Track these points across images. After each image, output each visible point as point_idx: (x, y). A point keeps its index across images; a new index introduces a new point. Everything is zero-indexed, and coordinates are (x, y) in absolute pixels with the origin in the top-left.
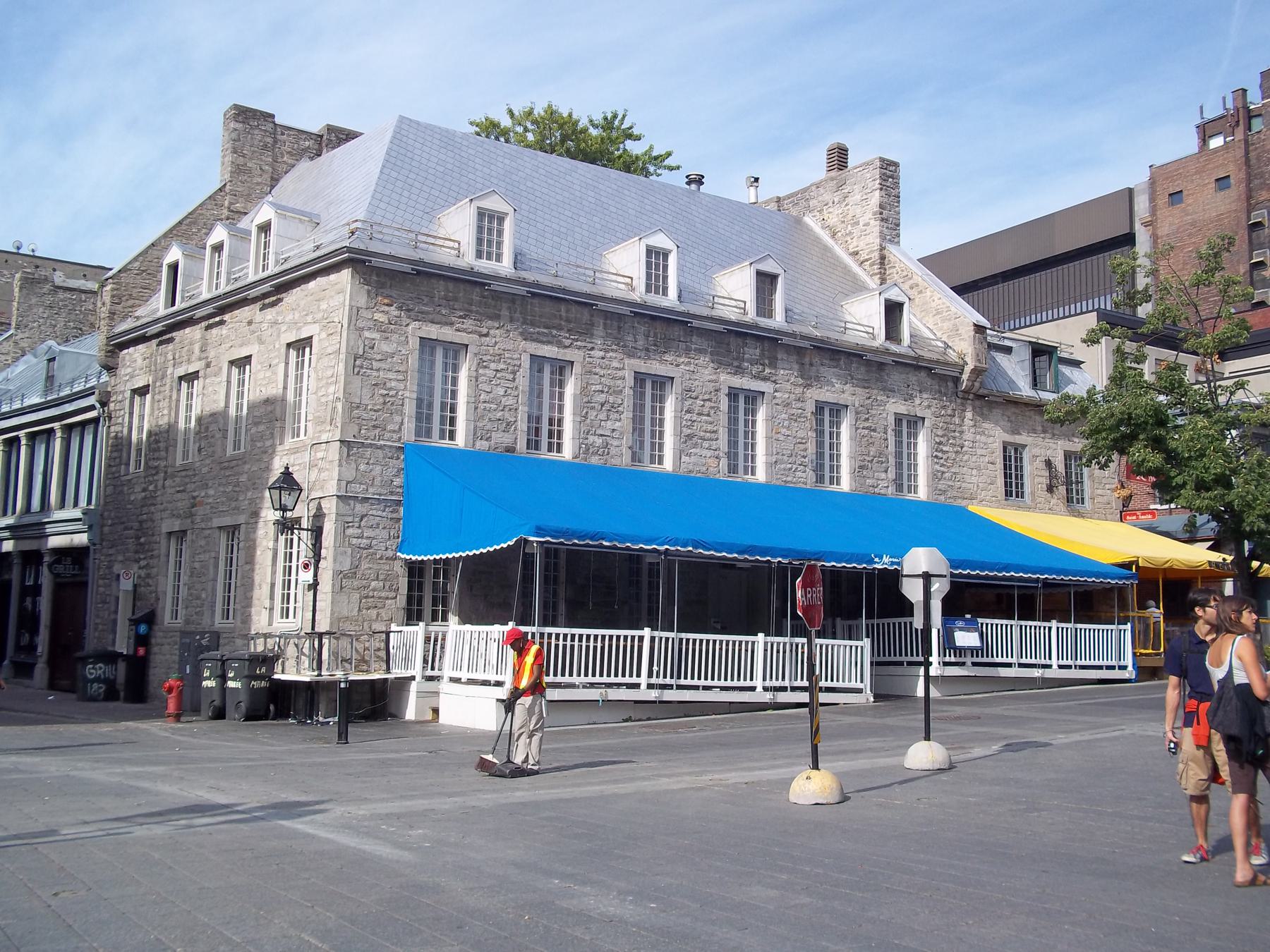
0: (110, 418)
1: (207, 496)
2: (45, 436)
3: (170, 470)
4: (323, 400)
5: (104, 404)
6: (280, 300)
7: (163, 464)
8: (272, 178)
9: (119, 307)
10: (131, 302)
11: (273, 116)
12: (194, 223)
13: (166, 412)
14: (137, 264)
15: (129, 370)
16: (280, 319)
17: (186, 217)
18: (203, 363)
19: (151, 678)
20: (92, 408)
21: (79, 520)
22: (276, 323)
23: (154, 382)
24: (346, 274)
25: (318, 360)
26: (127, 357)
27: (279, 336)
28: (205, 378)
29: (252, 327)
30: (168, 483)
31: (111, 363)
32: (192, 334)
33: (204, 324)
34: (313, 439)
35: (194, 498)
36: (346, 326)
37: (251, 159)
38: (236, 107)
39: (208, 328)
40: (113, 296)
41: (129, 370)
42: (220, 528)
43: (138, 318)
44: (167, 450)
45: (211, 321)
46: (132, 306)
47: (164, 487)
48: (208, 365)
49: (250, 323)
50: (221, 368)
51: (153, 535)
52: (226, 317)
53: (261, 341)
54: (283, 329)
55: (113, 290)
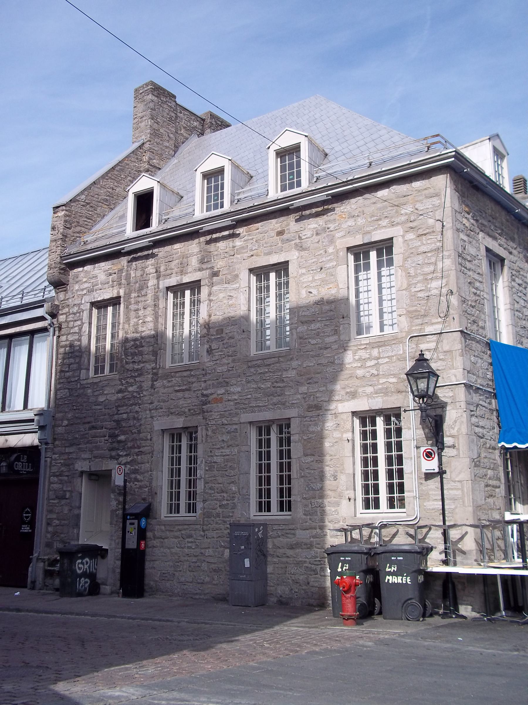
0: (60, 328)
1: (228, 393)
2: (6, 341)
3: (160, 371)
4: (421, 295)
5: (54, 315)
6: (333, 210)
7: (149, 366)
8: (175, 146)
9: (70, 232)
10: (78, 229)
11: (174, 97)
12: (122, 170)
13: (149, 319)
14: (83, 197)
15: (86, 285)
16: (332, 226)
17: (117, 165)
18: (206, 273)
19: (148, 571)
20: (42, 319)
21: (32, 421)
22: (325, 229)
23: (128, 295)
24: (442, 182)
25: (405, 259)
26: (82, 275)
27: (332, 241)
28: (212, 285)
29: (285, 236)
30: (157, 384)
31: (63, 278)
32: (193, 247)
33: (208, 238)
34: (408, 333)
35: (203, 395)
36: (448, 223)
37: (162, 126)
38: (152, 83)
39: (208, 243)
40: (66, 221)
41: (86, 285)
42: (250, 423)
43: (85, 243)
44: (155, 353)
45: (214, 236)
46: (79, 233)
47: (153, 387)
48: (216, 274)
49: (280, 233)
50: (237, 276)
51: (139, 432)
52: (240, 230)
53: (301, 248)
54: (338, 235)
55: (66, 215)
